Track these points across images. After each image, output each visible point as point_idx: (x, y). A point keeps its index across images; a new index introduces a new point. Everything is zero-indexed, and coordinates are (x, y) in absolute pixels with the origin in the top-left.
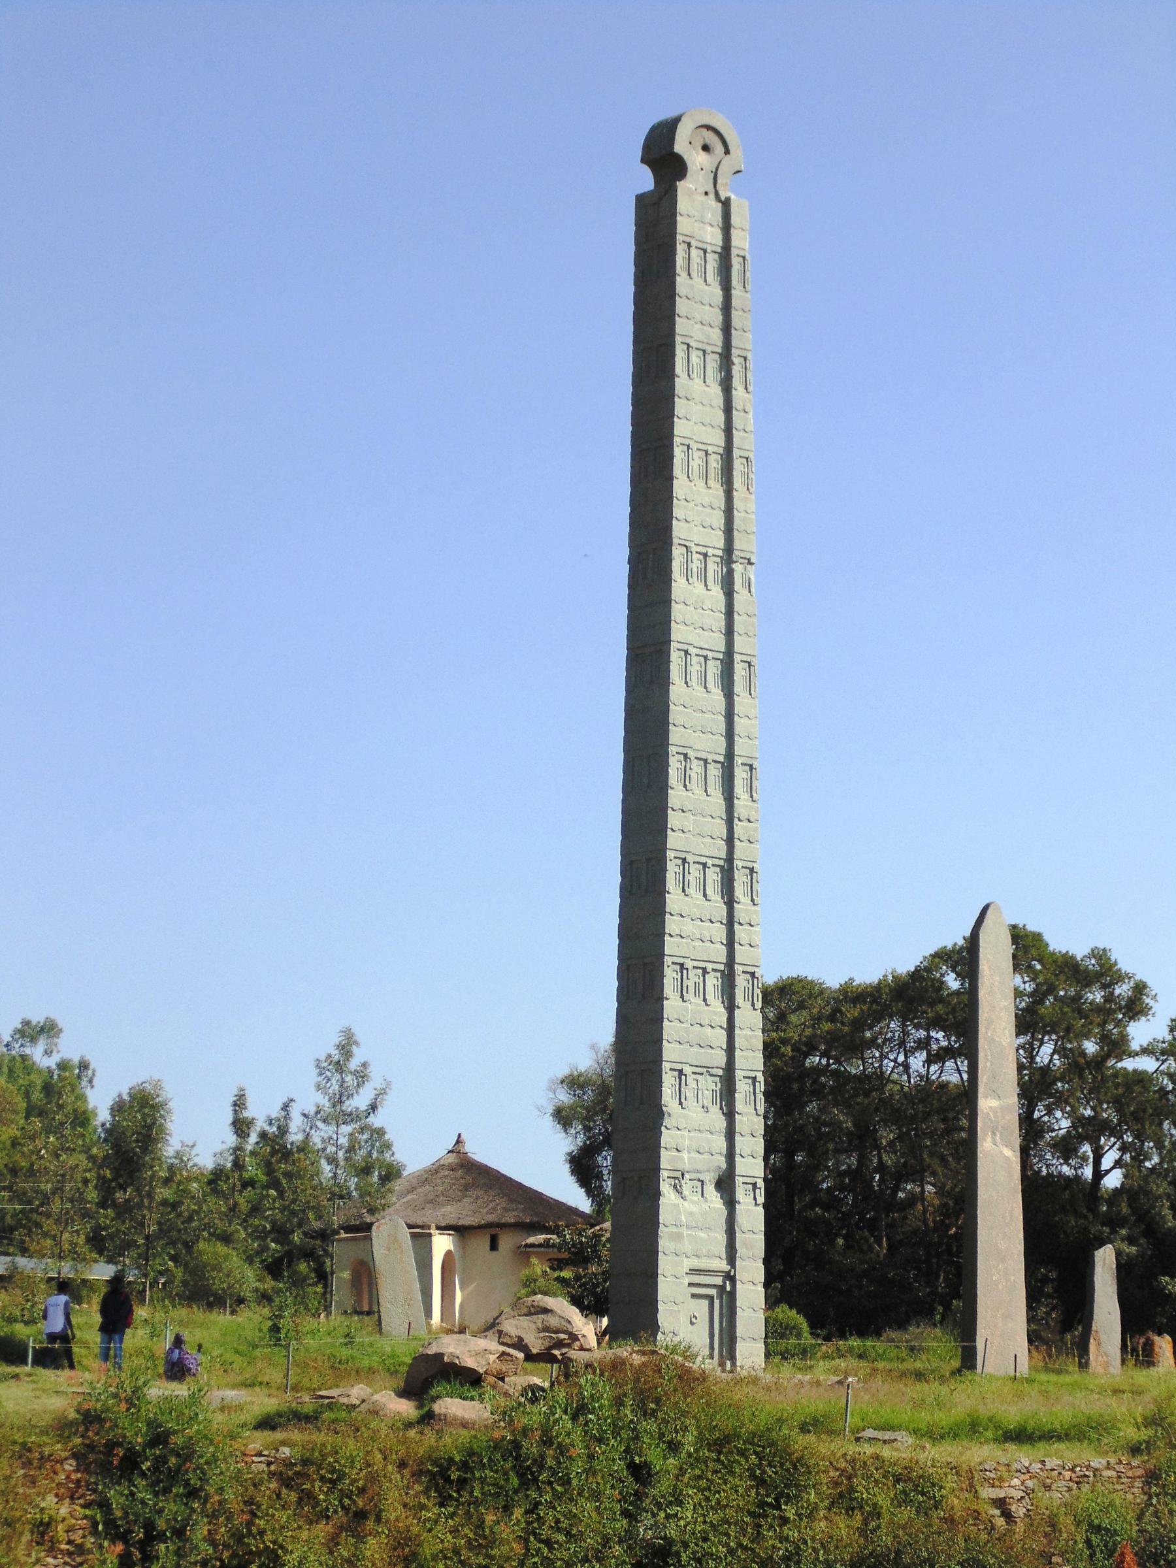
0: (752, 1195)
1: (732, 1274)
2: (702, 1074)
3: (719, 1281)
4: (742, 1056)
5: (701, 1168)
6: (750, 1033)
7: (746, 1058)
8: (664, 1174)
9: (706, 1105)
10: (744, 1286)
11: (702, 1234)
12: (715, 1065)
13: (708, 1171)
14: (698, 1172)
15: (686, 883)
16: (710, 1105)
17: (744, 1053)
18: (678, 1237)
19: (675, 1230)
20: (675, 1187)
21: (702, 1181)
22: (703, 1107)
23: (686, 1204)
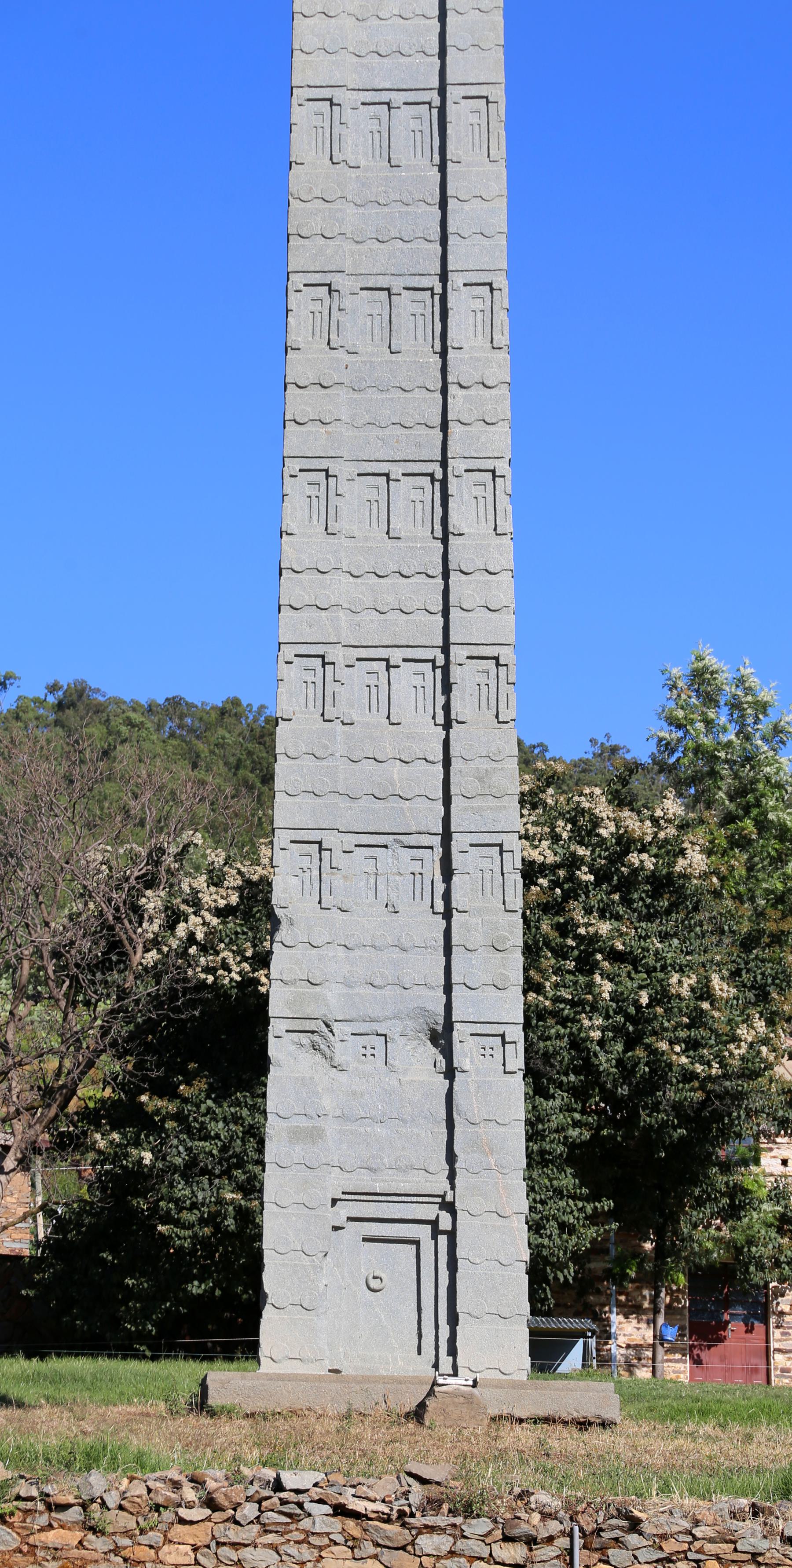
0: (499, 1057)
1: (449, 1198)
2: (386, 847)
3: (430, 1212)
4: (466, 809)
5: (375, 1011)
6: (486, 765)
7: (478, 811)
8: (276, 1027)
9: (393, 897)
10: (476, 1221)
11: (379, 1129)
12: (414, 829)
13: (397, 1017)
14: (372, 1021)
15: (332, 512)
16: (403, 902)
17: (475, 803)
18: (314, 1135)
19: (304, 1123)
20: (315, 1047)
21: (385, 1036)
22: (386, 906)
23: (343, 1078)
